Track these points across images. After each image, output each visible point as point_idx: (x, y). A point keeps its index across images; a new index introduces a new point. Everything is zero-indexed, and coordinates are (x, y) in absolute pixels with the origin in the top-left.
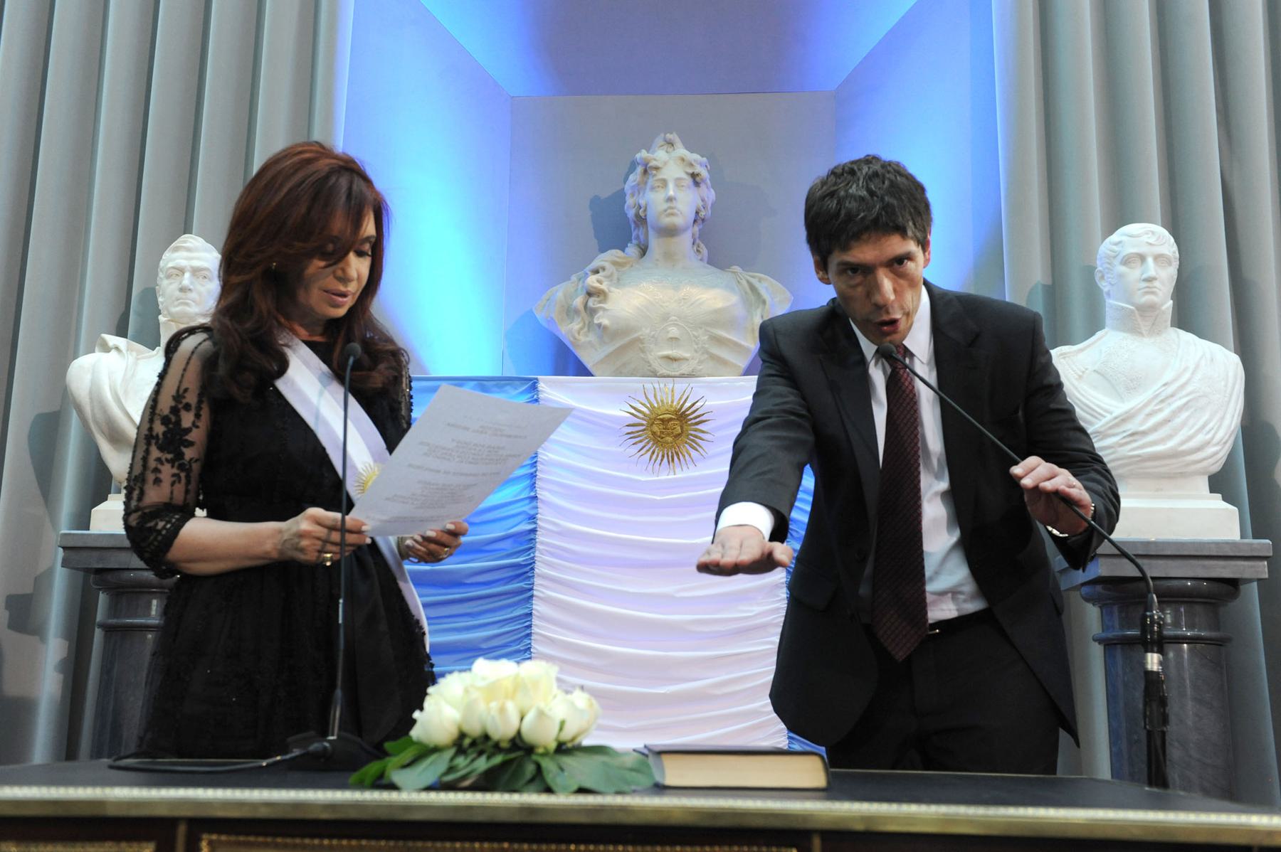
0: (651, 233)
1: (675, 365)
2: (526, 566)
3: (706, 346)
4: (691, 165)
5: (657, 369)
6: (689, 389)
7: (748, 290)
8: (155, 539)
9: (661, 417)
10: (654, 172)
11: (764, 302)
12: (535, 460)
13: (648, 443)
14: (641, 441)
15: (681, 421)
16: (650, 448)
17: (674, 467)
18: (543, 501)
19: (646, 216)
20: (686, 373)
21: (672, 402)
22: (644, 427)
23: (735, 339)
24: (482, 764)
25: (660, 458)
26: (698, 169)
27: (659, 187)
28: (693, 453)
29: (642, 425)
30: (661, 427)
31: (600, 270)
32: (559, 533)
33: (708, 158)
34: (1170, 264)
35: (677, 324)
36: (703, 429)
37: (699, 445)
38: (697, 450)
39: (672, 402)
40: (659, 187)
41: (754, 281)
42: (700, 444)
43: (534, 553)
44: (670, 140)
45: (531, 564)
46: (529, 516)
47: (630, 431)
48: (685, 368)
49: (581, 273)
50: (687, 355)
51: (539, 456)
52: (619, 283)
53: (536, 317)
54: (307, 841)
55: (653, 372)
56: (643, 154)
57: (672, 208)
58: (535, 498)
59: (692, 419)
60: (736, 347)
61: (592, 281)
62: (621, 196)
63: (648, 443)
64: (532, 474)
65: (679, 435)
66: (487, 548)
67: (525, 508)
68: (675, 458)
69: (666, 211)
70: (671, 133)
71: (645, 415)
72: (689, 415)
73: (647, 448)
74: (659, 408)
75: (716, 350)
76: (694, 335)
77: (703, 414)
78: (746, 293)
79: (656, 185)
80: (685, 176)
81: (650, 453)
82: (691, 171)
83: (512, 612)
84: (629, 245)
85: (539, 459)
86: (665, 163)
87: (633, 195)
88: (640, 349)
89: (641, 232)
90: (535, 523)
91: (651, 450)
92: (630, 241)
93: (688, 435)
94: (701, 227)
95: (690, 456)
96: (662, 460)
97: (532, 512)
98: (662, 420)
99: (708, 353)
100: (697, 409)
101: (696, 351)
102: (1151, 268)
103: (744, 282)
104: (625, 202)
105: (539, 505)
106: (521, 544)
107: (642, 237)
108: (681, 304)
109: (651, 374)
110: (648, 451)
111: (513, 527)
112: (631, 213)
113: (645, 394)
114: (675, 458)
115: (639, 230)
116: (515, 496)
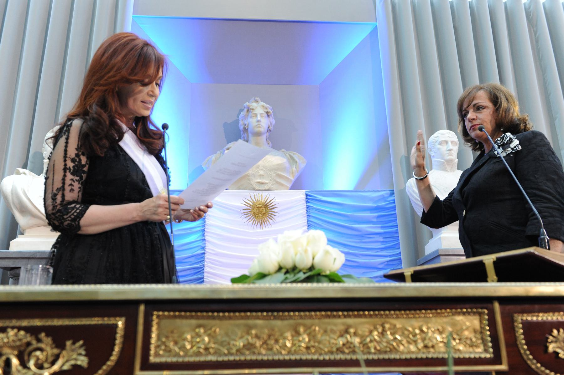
0: (250, 135)
1: (262, 185)
2: (201, 268)
3: (275, 178)
4: (266, 108)
5: (255, 187)
6: (268, 195)
7: (290, 158)
8: (75, 212)
9: (257, 206)
10: (252, 111)
11: (296, 162)
12: (204, 224)
13: (251, 217)
14: (249, 216)
16: (253, 219)
17: (262, 226)
18: (208, 241)
19: (248, 128)
21: (262, 200)
22: (250, 211)
23: (287, 176)
24: (302, 276)
26: (269, 110)
28: (270, 221)
29: (250, 209)
30: (257, 210)
33: (272, 107)
34: (456, 145)
36: (274, 211)
38: (272, 220)
39: (262, 200)
41: (292, 155)
43: (204, 262)
44: (257, 100)
45: (203, 267)
46: (202, 247)
47: (244, 212)
48: (266, 187)
49: (222, 150)
50: (267, 182)
51: (206, 222)
55: (253, 188)
56: (247, 103)
57: (259, 125)
60: (286, 179)
62: (237, 121)
63: (251, 217)
64: (203, 230)
65: (264, 214)
66: (184, 261)
67: (200, 244)
68: (263, 223)
69: (257, 126)
70: (257, 97)
71: (250, 205)
72: (269, 205)
75: (279, 180)
76: (270, 175)
78: (289, 159)
79: (253, 115)
80: (264, 112)
81: (252, 221)
82: (266, 111)
85: (206, 224)
86: (256, 107)
88: (248, 179)
89: (245, 135)
90: (205, 250)
91: (253, 220)
95: (269, 222)
96: (257, 224)
97: (203, 246)
98: (258, 207)
99: (275, 180)
100: (272, 203)
101: (271, 180)
102: (450, 146)
103: (288, 156)
105: (206, 242)
106: (199, 259)
107: (246, 137)
108: (264, 162)
109: (252, 189)
110: (251, 220)
111: (194, 253)
112: (241, 128)
113: (251, 197)
114: (263, 223)
115: (244, 134)
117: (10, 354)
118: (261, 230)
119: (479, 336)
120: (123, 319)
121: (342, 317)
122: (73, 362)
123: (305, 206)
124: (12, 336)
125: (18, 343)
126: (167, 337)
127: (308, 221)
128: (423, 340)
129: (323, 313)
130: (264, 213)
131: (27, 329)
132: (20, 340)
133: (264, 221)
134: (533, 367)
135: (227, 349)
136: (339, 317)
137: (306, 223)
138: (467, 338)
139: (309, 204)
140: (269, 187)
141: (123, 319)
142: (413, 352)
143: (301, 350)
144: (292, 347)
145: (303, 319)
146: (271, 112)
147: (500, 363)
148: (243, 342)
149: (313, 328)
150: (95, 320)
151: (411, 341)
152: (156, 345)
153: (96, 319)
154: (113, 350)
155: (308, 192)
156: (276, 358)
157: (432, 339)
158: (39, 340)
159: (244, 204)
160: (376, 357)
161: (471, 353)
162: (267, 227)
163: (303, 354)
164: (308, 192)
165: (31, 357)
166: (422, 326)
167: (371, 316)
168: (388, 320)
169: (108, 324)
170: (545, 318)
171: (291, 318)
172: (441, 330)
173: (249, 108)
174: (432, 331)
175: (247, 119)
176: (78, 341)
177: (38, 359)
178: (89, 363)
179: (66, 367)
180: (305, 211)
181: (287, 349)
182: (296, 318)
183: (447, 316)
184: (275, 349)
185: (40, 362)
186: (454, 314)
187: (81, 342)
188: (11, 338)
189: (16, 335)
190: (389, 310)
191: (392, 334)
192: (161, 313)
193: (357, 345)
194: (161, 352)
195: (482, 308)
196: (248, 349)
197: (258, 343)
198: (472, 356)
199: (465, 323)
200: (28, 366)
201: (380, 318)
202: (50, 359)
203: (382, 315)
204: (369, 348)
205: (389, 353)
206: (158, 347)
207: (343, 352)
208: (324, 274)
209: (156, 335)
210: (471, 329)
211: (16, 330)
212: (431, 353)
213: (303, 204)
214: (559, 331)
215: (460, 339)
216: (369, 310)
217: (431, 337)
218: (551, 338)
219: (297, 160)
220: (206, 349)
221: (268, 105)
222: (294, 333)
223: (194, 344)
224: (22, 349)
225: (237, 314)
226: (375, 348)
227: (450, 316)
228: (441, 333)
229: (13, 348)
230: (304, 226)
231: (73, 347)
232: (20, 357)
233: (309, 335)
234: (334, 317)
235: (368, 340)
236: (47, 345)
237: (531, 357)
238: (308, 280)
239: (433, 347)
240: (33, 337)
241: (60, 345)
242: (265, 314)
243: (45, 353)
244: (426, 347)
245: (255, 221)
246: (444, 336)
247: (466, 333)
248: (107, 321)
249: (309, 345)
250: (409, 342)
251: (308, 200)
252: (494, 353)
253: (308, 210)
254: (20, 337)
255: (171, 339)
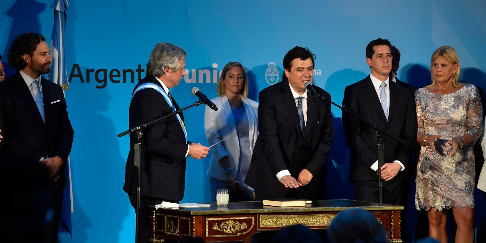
158: (236, 223)
241: (241, 223)
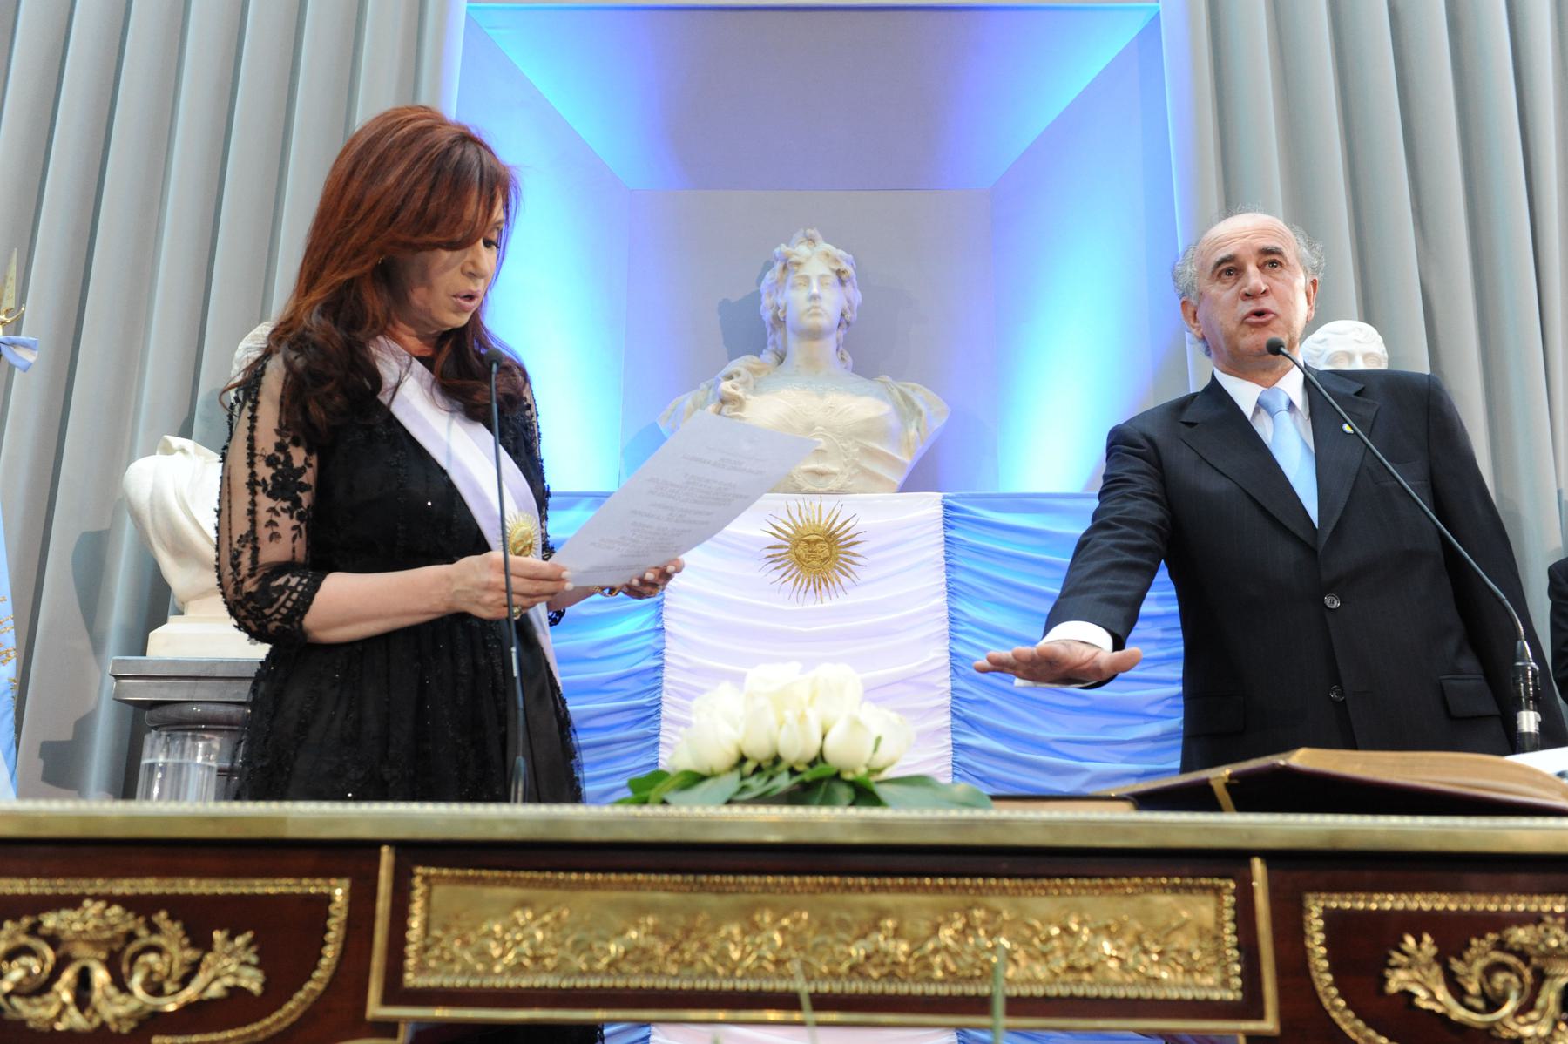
0: (791, 337)
1: (822, 480)
3: (857, 459)
4: (836, 261)
5: (802, 484)
7: (902, 403)
9: (807, 538)
10: (796, 268)
11: (920, 413)
13: (792, 567)
14: (784, 566)
15: (829, 543)
16: (794, 574)
18: (671, 634)
19: (784, 318)
20: (834, 489)
21: (820, 521)
22: (784, 550)
24: (783, 782)
25: (805, 585)
26: (844, 266)
27: (801, 284)
28: (844, 580)
29: (786, 547)
30: (807, 549)
31: (735, 376)
32: (689, 671)
35: (825, 436)
37: (851, 571)
38: (847, 575)
39: (820, 521)
40: (801, 284)
41: (908, 391)
42: (853, 569)
46: (653, 651)
47: (770, 554)
48: (833, 484)
49: (712, 381)
50: (835, 469)
52: (756, 390)
53: (661, 432)
54: (561, 876)
56: (783, 248)
58: (662, 629)
59: (841, 541)
60: (890, 461)
61: (726, 386)
62: (756, 297)
63: (792, 567)
64: (658, 603)
68: (823, 586)
69: (809, 310)
72: (839, 535)
73: (791, 573)
74: (804, 528)
75: (867, 464)
76: (846, 450)
77: (855, 535)
79: (799, 282)
80: (828, 272)
82: (836, 267)
83: (634, 762)
84: (764, 351)
86: (808, 259)
87: (770, 295)
89: (778, 336)
91: (795, 576)
92: (765, 346)
93: (837, 559)
94: (845, 332)
95: (840, 583)
96: (807, 587)
97: (658, 647)
98: (808, 542)
99: (857, 465)
100: (848, 529)
101: (846, 465)
104: (761, 303)
105: (667, 638)
106: (645, 683)
107: (779, 343)
108: (829, 411)
110: (791, 577)
112: (767, 316)
113: (789, 512)
114: (823, 586)
116: (637, 629)
117: (89, 958)
118: (819, 605)
119: (1208, 945)
120: (346, 882)
121: (866, 889)
122: (229, 981)
123: (942, 539)
124: (94, 915)
125: (107, 935)
126: (446, 928)
127: (949, 581)
128: (1067, 952)
129: (821, 879)
130: (827, 558)
131: (128, 903)
132: (112, 927)
133: (825, 580)
134: (1345, 1027)
135: (587, 961)
136: (860, 889)
137: (944, 586)
138: (1179, 951)
139: (951, 533)
140: (840, 485)
141: (346, 882)
142: (1038, 982)
143: (765, 969)
144: (742, 959)
145: (769, 892)
146: (850, 270)
147: (1260, 1016)
148: (624, 944)
149: (796, 914)
150: (281, 885)
151: (1037, 954)
152: (420, 944)
153: (284, 881)
154: (320, 956)
155: (949, 498)
156: (701, 984)
157: (1088, 949)
158: (154, 929)
159: (771, 533)
160: (943, 990)
161: (1185, 987)
162: (834, 596)
163: (767, 978)
164: (949, 498)
165: (136, 967)
166: (1067, 916)
167: (939, 890)
168: (979, 899)
169: (309, 895)
170: (1388, 906)
171: (741, 889)
172: (1113, 929)
173: (786, 260)
174: (1091, 930)
175: (783, 292)
176: (241, 932)
177: (151, 972)
178: (265, 985)
179: (215, 990)
180: (939, 552)
181: (729, 964)
182: (753, 889)
183: (1132, 894)
184: (699, 967)
185: (156, 978)
186: (1149, 889)
187: (249, 935)
188: (90, 926)
189: (102, 915)
190: (985, 876)
191: (991, 935)
192: (433, 871)
193: (902, 959)
194: (432, 963)
195: (1221, 877)
196: (637, 962)
197: (660, 949)
198: (1188, 995)
199: (1175, 911)
200: (129, 986)
201: (960, 894)
202: (178, 972)
203: (966, 888)
204: (929, 967)
205: (977, 981)
206: (426, 949)
207: (865, 977)
208: (849, 776)
209: (420, 922)
210: (1192, 930)
211: (101, 905)
212: (1084, 984)
213: (936, 532)
214: (1419, 941)
215: (1160, 954)
216: (933, 875)
217: (1086, 944)
218: (1397, 957)
219: (921, 406)
220: (536, 959)
221: (841, 252)
222: (747, 927)
223: (509, 945)
224: (116, 947)
225: (613, 877)
226: (944, 968)
227: (1139, 893)
228: (1112, 937)
229: (95, 944)
230: (937, 595)
231: (230, 947)
232: (112, 965)
233: (783, 930)
234: (848, 888)
235: (930, 946)
236: (170, 939)
237: (1341, 1003)
238: (793, 798)
239: (1090, 969)
240: (141, 920)
242: (678, 878)
243: (166, 959)
244: (1071, 968)
245: (801, 579)
246: (1121, 942)
247: (1180, 941)
248: (312, 887)
249: (783, 955)
250: (1030, 956)
251: (951, 522)
252: (1242, 989)
253: (948, 549)
254: (114, 921)
255: (455, 932)
